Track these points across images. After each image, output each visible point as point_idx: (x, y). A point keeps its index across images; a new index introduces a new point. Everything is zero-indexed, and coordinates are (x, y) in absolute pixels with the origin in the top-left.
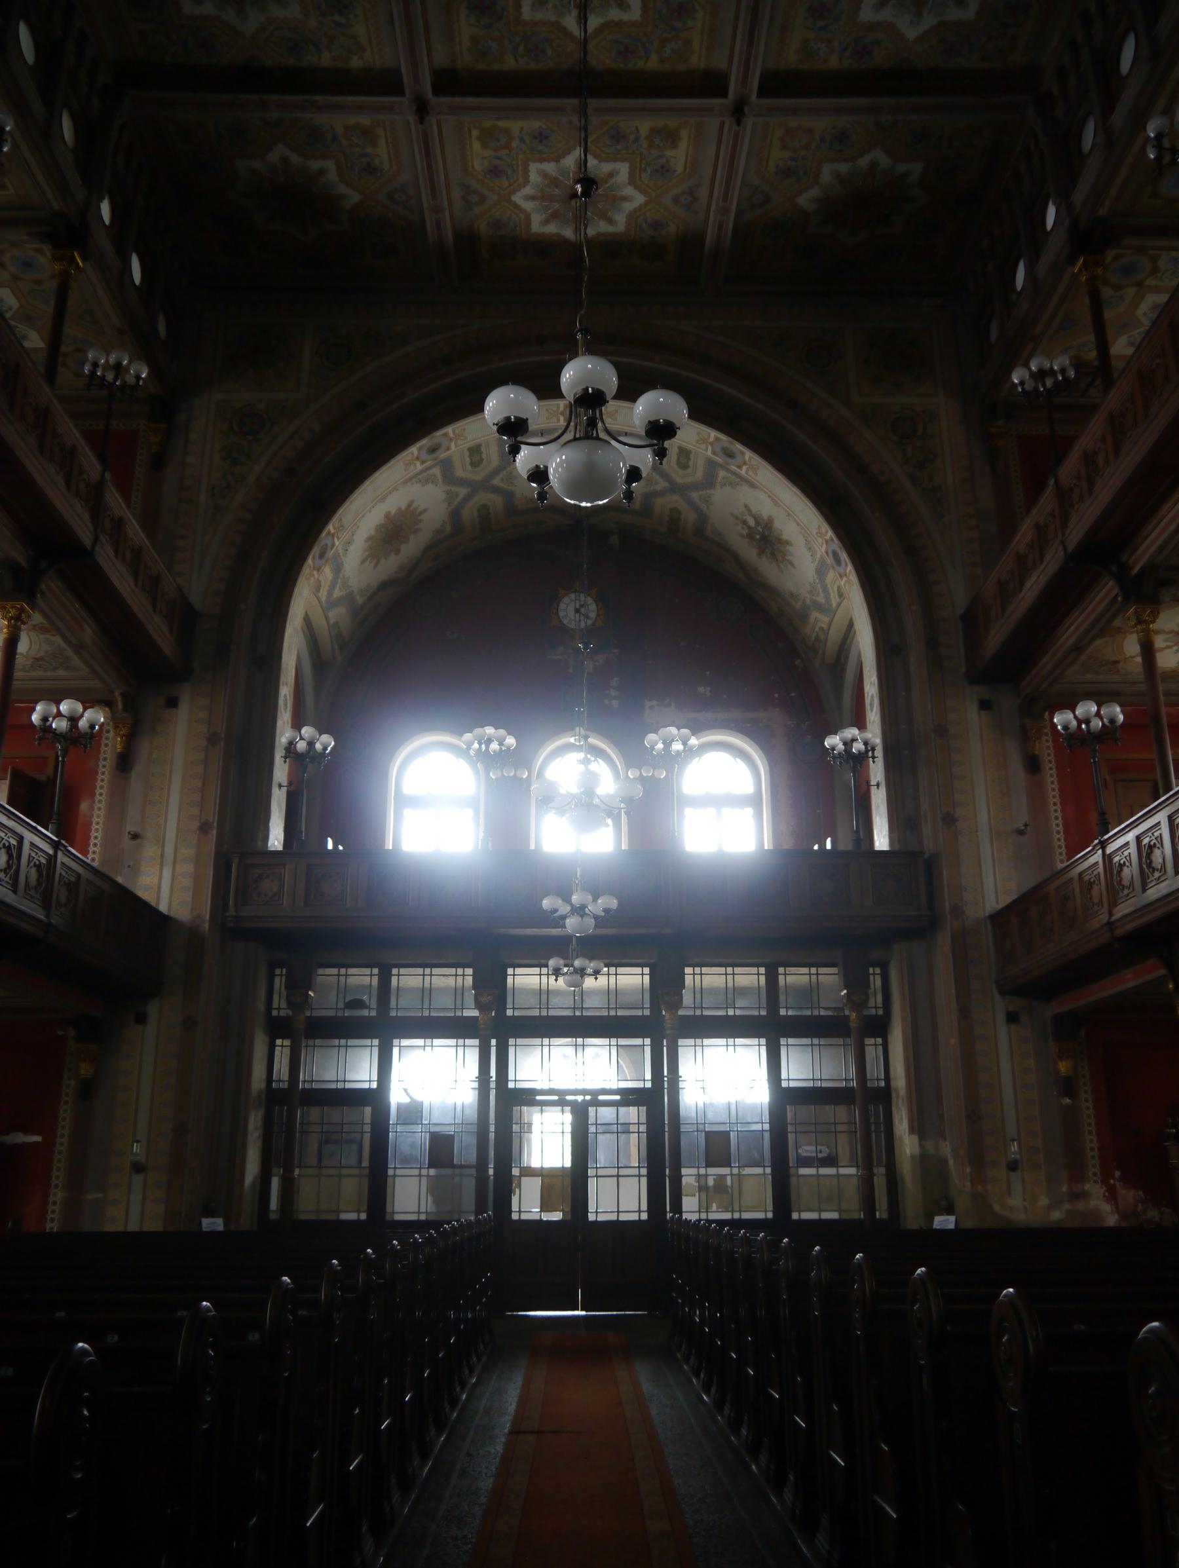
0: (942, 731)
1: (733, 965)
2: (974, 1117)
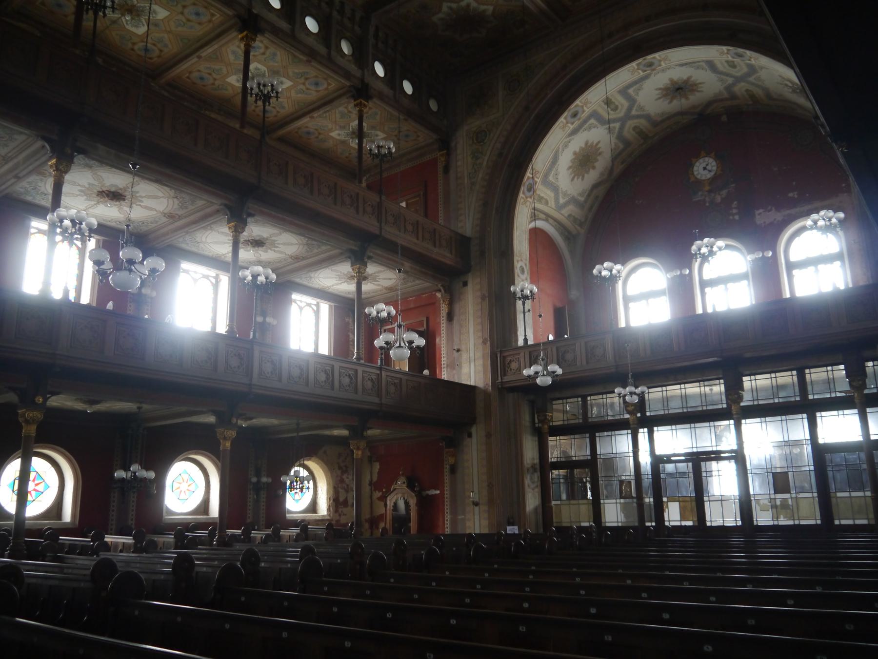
1: (775, 372)
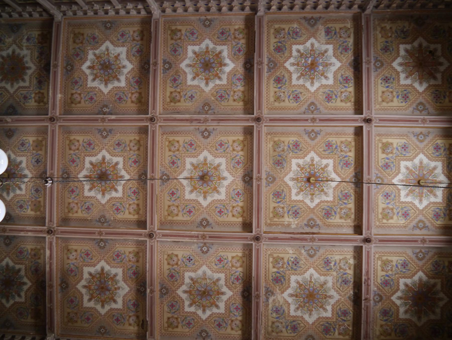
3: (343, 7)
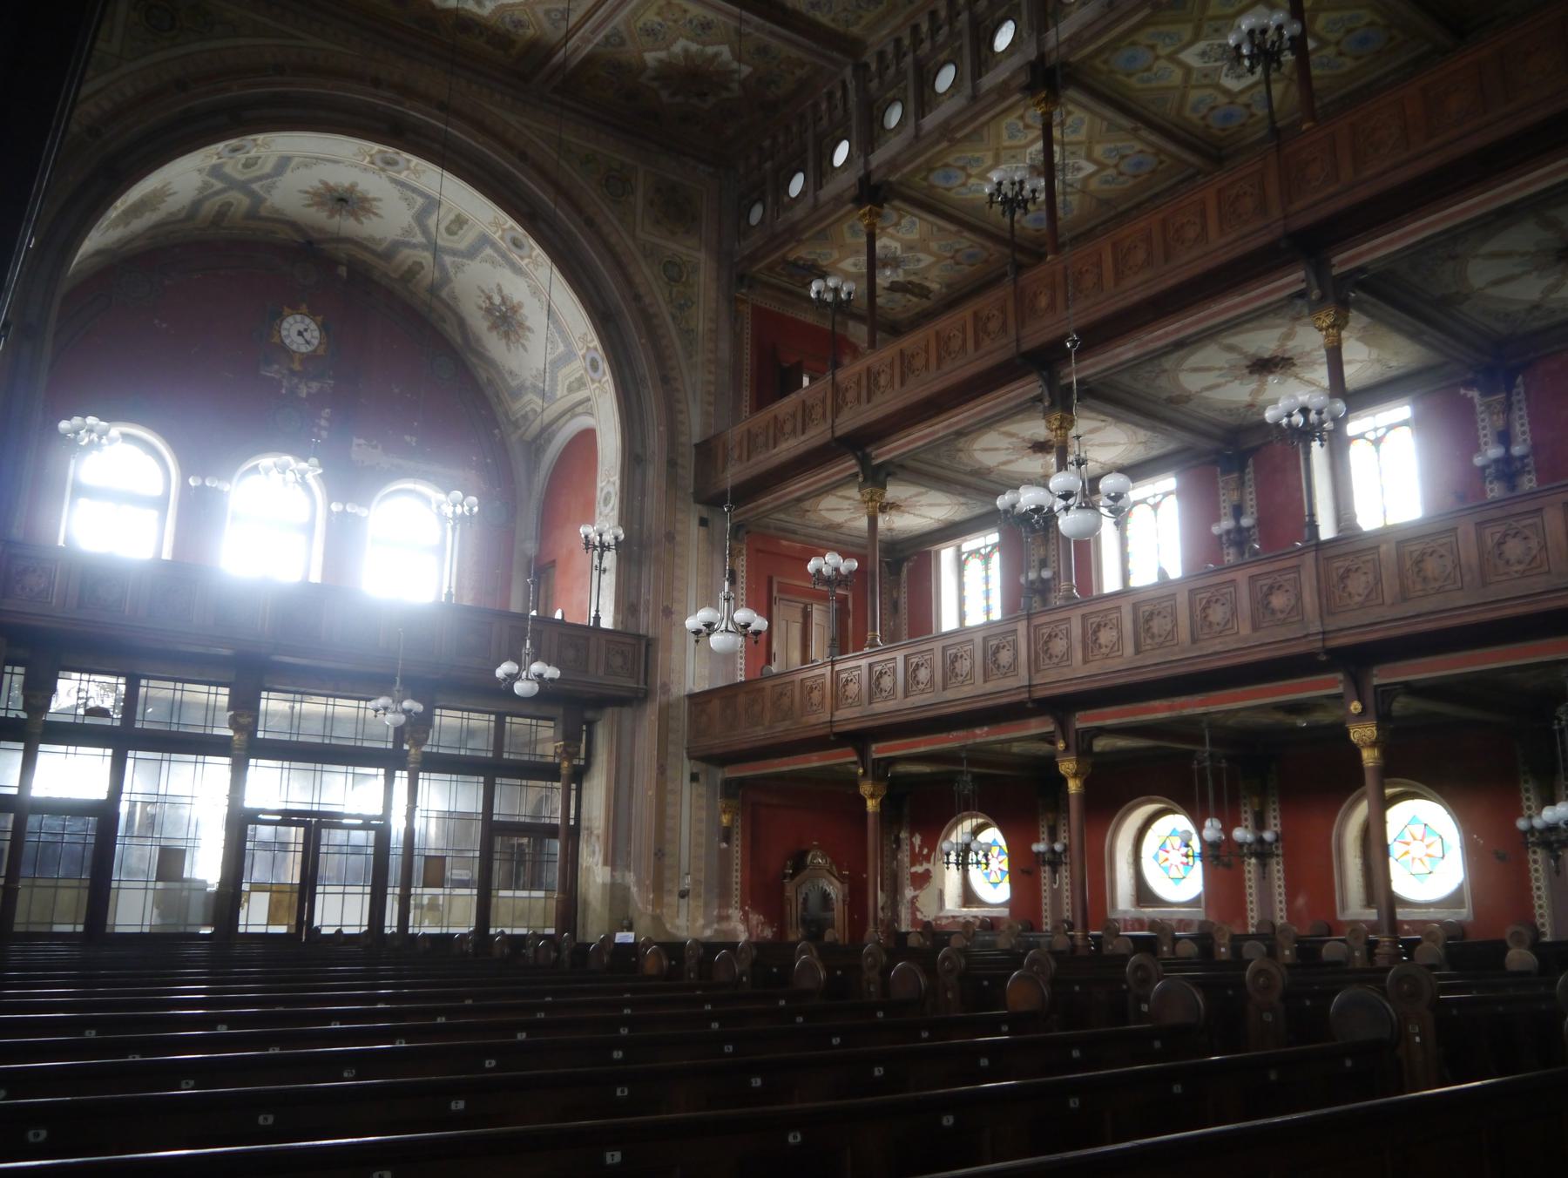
0: (670, 537)
2: (660, 854)
3: (890, 49)
